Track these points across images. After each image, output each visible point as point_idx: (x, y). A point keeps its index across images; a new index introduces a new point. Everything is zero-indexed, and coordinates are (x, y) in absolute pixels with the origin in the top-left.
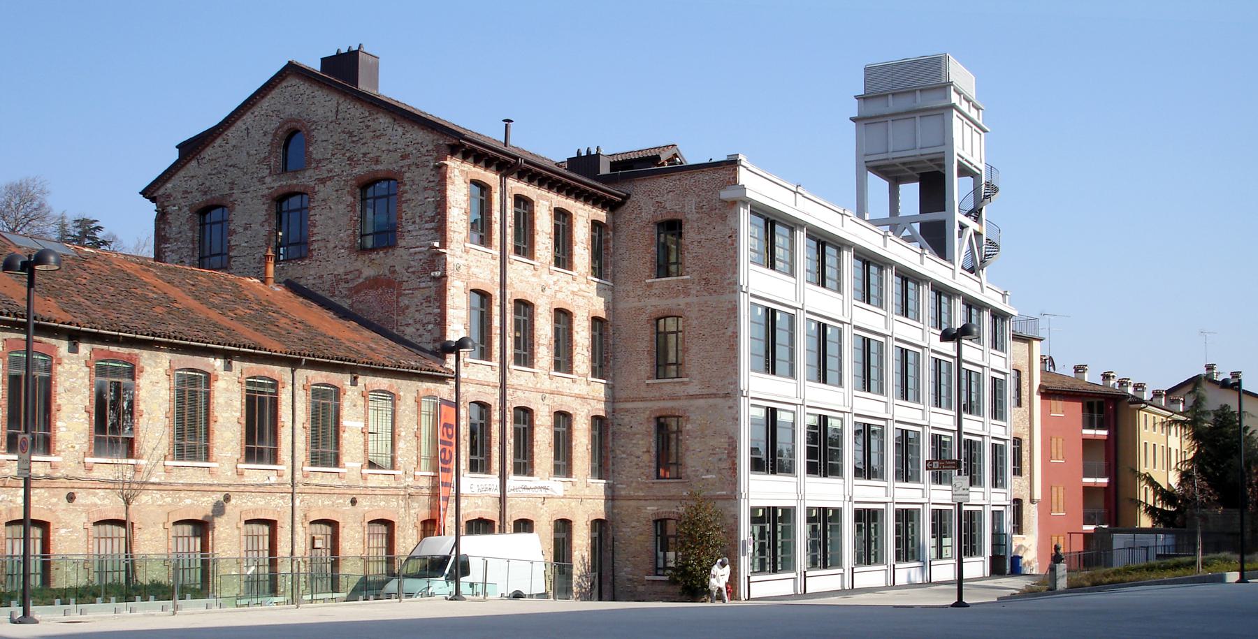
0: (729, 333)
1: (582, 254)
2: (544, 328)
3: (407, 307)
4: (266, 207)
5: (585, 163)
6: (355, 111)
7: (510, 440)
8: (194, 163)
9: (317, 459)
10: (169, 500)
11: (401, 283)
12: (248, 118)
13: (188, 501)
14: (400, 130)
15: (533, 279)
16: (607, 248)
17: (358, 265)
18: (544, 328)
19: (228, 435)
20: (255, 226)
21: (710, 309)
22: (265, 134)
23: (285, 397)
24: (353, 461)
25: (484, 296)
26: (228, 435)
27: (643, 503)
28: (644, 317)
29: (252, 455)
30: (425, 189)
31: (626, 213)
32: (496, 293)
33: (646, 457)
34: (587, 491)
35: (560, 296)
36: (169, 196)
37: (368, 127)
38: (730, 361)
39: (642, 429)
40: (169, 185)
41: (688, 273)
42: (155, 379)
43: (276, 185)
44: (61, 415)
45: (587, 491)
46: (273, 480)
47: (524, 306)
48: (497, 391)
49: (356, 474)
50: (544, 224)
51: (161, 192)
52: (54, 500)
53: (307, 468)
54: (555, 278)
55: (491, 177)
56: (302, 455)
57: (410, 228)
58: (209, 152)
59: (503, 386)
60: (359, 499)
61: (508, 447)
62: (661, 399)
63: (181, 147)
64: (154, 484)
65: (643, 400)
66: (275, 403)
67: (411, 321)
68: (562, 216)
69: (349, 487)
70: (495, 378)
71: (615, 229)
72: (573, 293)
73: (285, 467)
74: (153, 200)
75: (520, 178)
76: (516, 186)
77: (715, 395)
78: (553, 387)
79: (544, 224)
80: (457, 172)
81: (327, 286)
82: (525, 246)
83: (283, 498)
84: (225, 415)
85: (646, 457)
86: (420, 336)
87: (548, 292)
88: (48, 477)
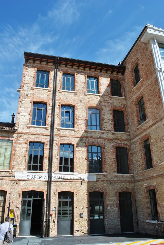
0: (157, 91)
21: (150, 86)
27: (143, 182)
28: (134, 103)
32: (51, 102)
34: (115, 179)
38: (160, 103)
39: (138, 148)
41: (141, 78)
45: (115, 179)
59: (52, 136)
61: (54, 159)
65: (137, 136)
70: (48, 132)
71: (124, 80)
77: (157, 122)
85: (141, 161)
87: (83, 101)
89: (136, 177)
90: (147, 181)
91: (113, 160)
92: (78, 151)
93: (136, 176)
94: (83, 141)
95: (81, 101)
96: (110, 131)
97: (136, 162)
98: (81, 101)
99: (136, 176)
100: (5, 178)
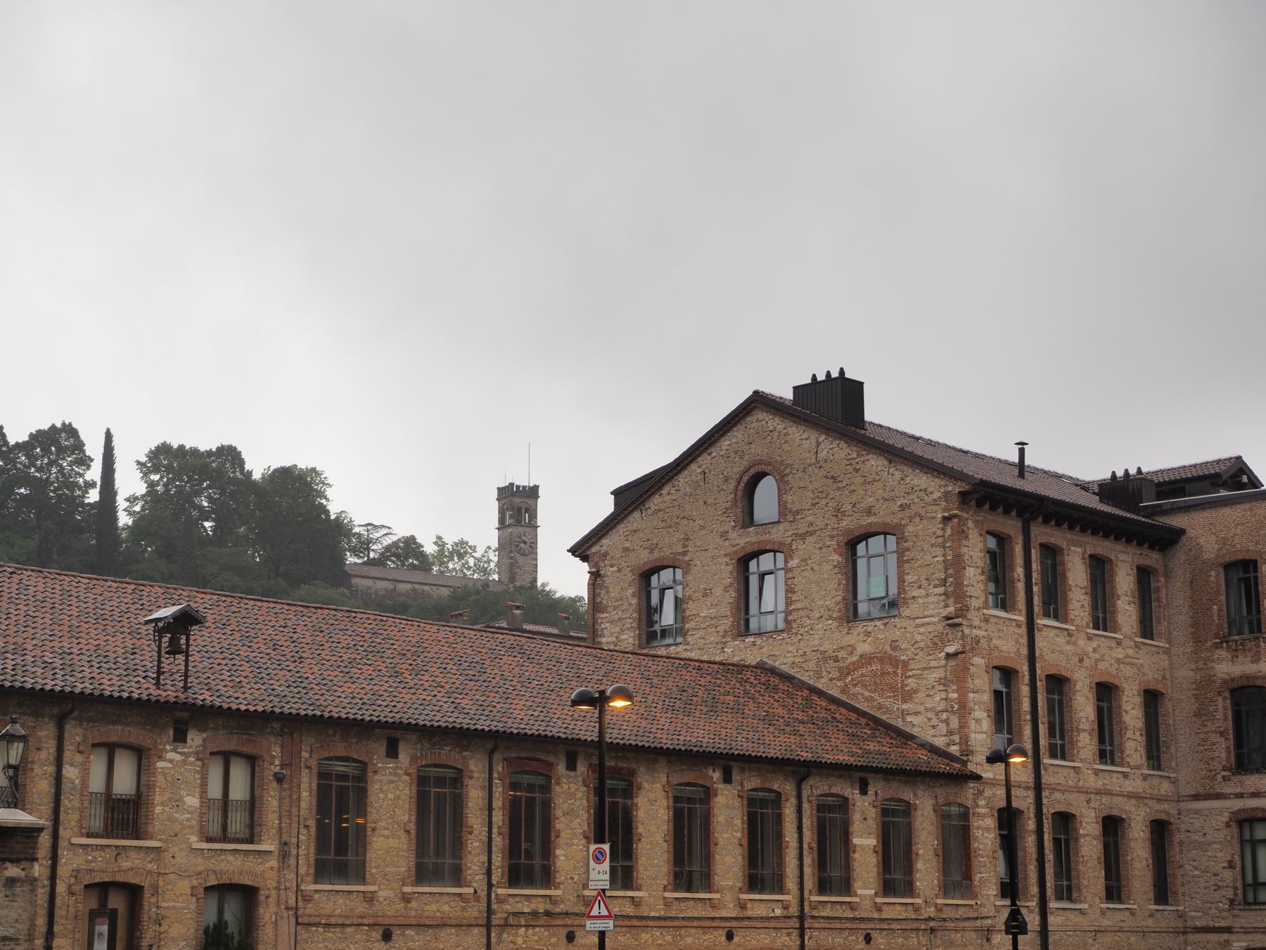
1: (1126, 610)
2: (1084, 708)
3: (916, 691)
4: (730, 568)
5: (1121, 489)
6: (836, 451)
7: (1050, 856)
8: (636, 514)
9: (824, 886)
10: (669, 938)
11: (905, 664)
12: (704, 460)
13: (689, 940)
14: (898, 475)
15: (1068, 648)
16: (1159, 600)
17: (850, 640)
18: (1084, 708)
19: (729, 859)
20: (718, 591)
22: (726, 479)
23: (789, 811)
24: (865, 887)
25: (1007, 674)
26: (729, 859)
29: (755, 882)
30: (933, 545)
31: (1180, 556)
32: (1025, 669)
33: (1228, 875)
35: (1101, 666)
36: (605, 555)
37: (857, 470)
40: (605, 541)
42: (652, 796)
43: (742, 542)
44: (561, 841)
45: (1150, 922)
46: (778, 912)
47: (1058, 683)
48: (1031, 794)
49: (867, 904)
50: (1077, 574)
51: (594, 549)
52: (554, 940)
53: (814, 898)
54: (1095, 644)
55: (1011, 526)
56: (809, 883)
57: (915, 594)
58: (655, 502)
60: (874, 935)
62: (1240, 796)
63: (617, 493)
64: (654, 918)
65: (1219, 796)
66: (779, 819)
67: (921, 709)
68: (1099, 569)
69: (862, 920)
72: (1118, 661)
73: (791, 898)
74: (584, 558)
75: (1046, 521)
76: (1042, 533)
78: (1099, 784)
79: (1077, 574)
80: (970, 524)
81: (812, 665)
82: (1055, 604)
83: (789, 934)
84: (725, 836)
86: (934, 727)
87: (1087, 662)
88: (548, 914)
89: (1192, 917)
90: (1249, 937)
91: (1145, 863)
92: (1084, 836)
93: (1193, 914)
94: (1092, 805)
95: (1081, 661)
96: (1138, 768)
97: (1196, 873)
98: (1081, 661)
99: (1193, 914)
100: (966, 924)
